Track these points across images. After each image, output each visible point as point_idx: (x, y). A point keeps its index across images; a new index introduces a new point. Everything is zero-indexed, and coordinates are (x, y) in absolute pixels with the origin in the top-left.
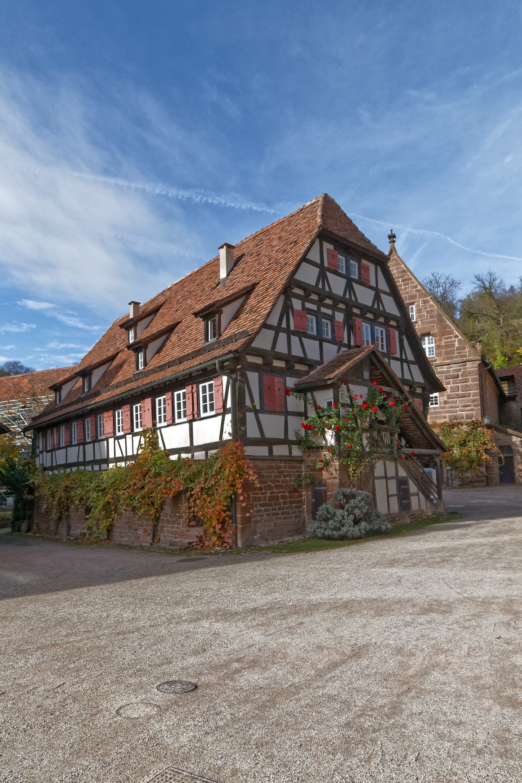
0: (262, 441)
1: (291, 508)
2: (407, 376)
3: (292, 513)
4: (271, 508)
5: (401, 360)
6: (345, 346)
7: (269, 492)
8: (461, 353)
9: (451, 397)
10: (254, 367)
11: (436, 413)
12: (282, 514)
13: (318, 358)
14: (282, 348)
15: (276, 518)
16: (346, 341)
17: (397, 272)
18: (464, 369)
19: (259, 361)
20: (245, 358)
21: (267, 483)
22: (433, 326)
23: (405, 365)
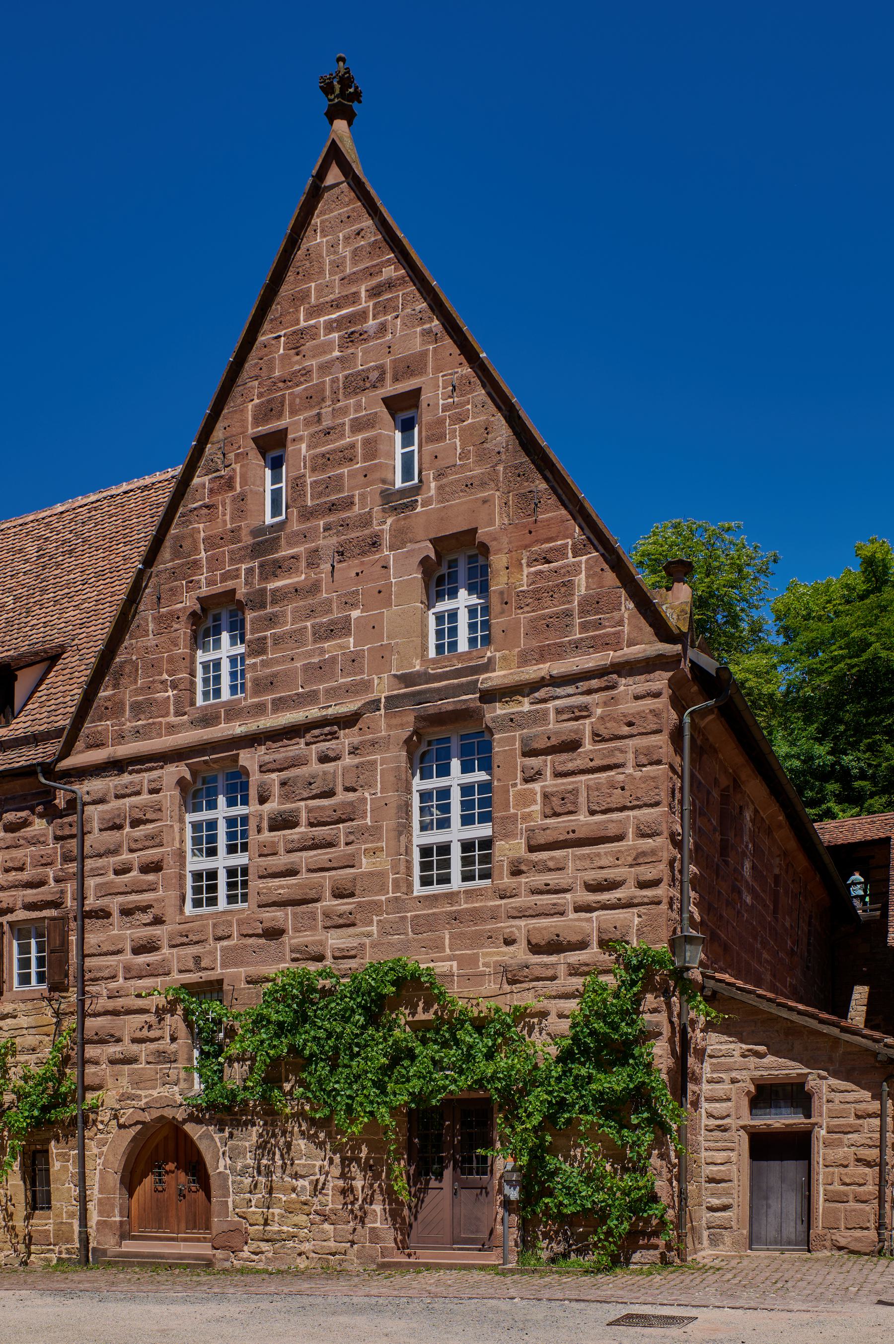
8: (599, 625)
9: (541, 839)
11: (475, 916)
17: (355, 253)
18: (605, 704)
22: (485, 501)
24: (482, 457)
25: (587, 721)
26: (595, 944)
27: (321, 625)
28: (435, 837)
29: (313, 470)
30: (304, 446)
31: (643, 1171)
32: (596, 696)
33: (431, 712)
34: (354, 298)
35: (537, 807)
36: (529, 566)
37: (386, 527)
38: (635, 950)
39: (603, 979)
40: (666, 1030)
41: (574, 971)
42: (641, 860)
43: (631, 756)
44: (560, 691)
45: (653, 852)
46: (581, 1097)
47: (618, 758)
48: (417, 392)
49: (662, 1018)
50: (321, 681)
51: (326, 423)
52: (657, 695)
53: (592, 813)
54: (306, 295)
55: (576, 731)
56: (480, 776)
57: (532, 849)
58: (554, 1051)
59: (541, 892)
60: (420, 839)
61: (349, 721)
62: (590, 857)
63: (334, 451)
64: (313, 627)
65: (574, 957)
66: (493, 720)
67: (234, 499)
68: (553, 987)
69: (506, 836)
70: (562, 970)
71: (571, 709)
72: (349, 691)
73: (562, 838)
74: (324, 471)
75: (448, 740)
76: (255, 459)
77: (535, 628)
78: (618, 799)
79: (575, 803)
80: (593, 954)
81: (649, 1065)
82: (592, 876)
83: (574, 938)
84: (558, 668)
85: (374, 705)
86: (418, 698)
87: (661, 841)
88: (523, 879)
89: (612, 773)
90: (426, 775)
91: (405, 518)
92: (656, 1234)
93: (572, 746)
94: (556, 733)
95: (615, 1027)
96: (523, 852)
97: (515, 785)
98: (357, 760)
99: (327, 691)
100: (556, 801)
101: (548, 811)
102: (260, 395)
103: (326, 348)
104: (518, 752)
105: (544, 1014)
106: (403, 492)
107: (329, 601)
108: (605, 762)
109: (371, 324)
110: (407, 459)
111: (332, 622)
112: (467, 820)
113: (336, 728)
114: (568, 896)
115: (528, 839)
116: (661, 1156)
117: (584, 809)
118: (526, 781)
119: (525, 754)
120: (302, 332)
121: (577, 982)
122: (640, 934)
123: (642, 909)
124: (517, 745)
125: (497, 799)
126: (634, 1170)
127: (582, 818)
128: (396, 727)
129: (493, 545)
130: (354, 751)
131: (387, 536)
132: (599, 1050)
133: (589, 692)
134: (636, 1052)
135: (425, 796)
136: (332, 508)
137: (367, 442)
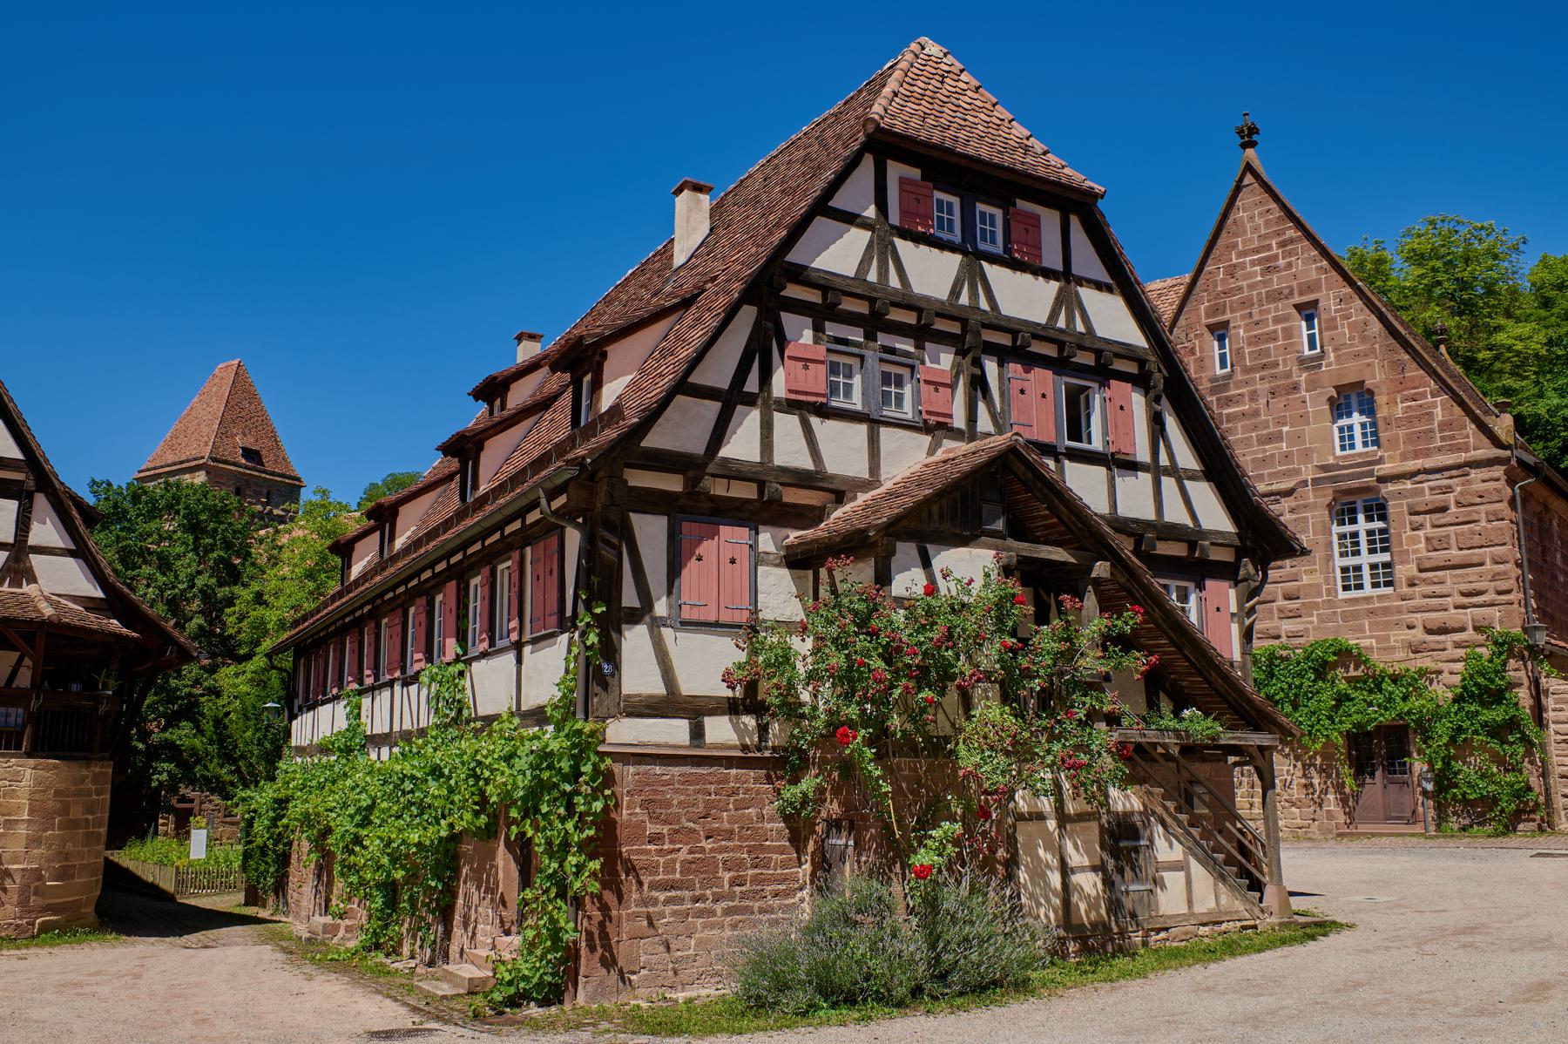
0: (668, 705)
1: (757, 895)
2: (1175, 513)
3: (762, 911)
4: (687, 894)
5: (1157, 471)
6: (956, 434)
7: (685, 849)
8: (1453, 437)
10: (654, 502)
12: (728, 912)
13: (865, 475)
14: (742, 445)
15: (705, 926)
16: (959, 422)
18: (1463, 484)
19: (673, 484)
20: (620, 477)
21: (678, 822)
22: (1369, 365)
23: (1168, 483)
24: (1364, 339)
25: (1451, 495)
26: (1471, 628)
27: (1263, 435)
28: (1351, 561)
29: (1250, 344)
30: (1241, 331)
31: (1520, 772)
32: (1456, 480)
33: (1344, 488)
34: (1269, 248)
35: (1422, 545)
36: (1402, 402)
37: (1303, 378)
38: (1499, 633)
39: (1478, 650)
40: (1526, 682)
41: (1458, 645)
42: (1497, 578)
43: (1483, 515)
44: (1431, 477)
45: (1505, 573)
46: (1472, 724)
47: (1475, 517)
48: (1316, 301)
49: (1522, 674)
50: (1265, 469)
51: (1256, 318)
52: (1497, 480)
53: (1461, 549)
54: (1235, 245)
55: (1445, 501)
56: (1380, 525)
57: (1421, 571)
58: (1450, 695)
59: (1430, 597)
60: (1339, 562)
61: (1288, 493)
62: (1461, 575)
63: (1262, 334)
64: (1257, 436)
65: (1457, 637)
66: (1387, 493)
67: (1196, 360)
68: (1444, 655)
69: (1402, 563)
70: (1449, 645)
71: (1440, 487)
72: (1285, 474)
73: (1441, 564)
74: (1257, 346)
75: (1354, 503)
76: (1208, 337)
77: (1409, 439)
78: (1477, 540)
79: (1448, 543)
80: (1470, 634)
81: (1516, 704)
82: (1465, 587)
83: (1456, 625)
84: (1429, 463)
85: (1304, 483)
86: (1334, 479)
87: (1510, 566)
88: (1417, 589)
89: (1472, 525)
90: (1341, 523)
91: (1315, 374)
92: (1533, 811)
93: (1443, 509)
94: (1431, 502)
95: (1492, 681)
96: (1415, 572)
97: (1405, 532)
98: (1294, 516)
99: (1270, 475)
100: (1435, 543)
101: (1431, 548)
102: (1209, 301)
103: (1254, 274)
104: (1406, 512)
105: (1439, 672)
106: (1312, 359)
107: (1267, 421)
108: (1467, 519)
109: (1281, 262)
110: (1311, 338)
111: (1270, 434)
112: (1372, 551)
113: (1278, 497)
114: (1449, 599)
115: (1418, 565)
116: (1531, 763)
117: (1454, 546)
118: (1413, 530)
119: (1411, 514)
120: (1235, 266)
121: (1461, 652)
122: (1501, 622)
123: (1501, 607)
124: (1405, 508)
125: (1394, 540)
126: (1513, 770)
127: (1454, 552)
128: (1321, 497)
129: (1376, 391)
130: (1292, 511)
131: (1303, 385)
132: (1481, 695)
133: (1451, 478)
134: (1507, 695)
135: (1342, 536)
136: (1264, 367)
137: (1284, 329)
